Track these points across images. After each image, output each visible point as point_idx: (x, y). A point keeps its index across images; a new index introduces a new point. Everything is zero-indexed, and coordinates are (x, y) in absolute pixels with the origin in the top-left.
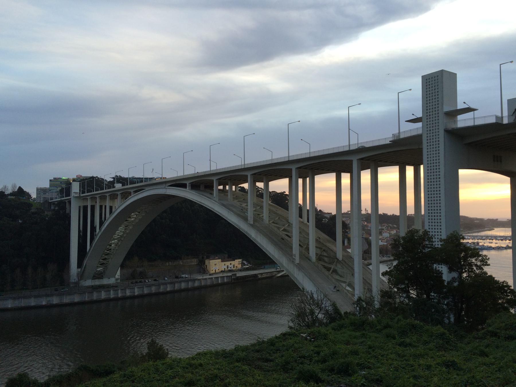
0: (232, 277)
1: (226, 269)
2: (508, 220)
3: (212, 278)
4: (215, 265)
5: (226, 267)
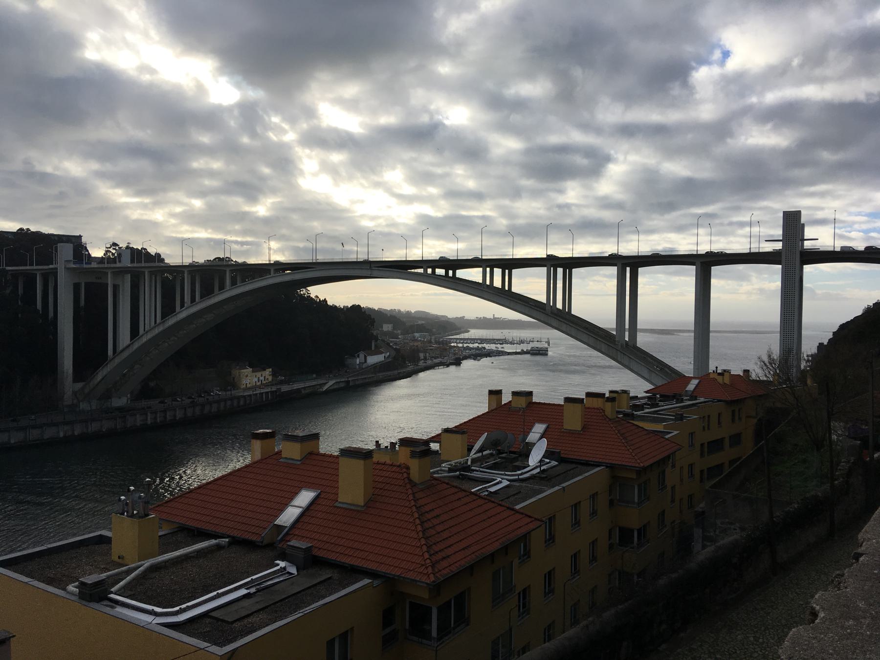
0: (276, 393)
1: (257, 382)
3: (257, 394)
4: (247, 376)
5: (256, 380)
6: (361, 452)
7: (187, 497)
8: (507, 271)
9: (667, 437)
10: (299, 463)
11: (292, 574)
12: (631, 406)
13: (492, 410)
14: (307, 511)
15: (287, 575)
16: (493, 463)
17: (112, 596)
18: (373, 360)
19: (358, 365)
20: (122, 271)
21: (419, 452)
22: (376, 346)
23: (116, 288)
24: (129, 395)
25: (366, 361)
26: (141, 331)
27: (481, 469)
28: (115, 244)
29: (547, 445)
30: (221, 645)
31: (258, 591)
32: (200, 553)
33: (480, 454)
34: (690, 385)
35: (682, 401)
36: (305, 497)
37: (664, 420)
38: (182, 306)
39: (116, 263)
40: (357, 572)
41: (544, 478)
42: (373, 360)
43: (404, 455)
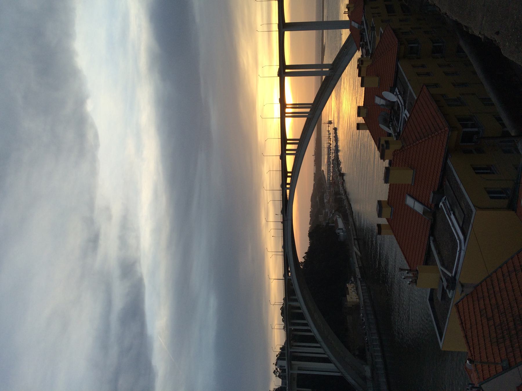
2: (315, 166)
6: (386, 171)
7: (411, 264)
8: (288, 142)
9: (382, 32)
10: (393, 208)
11: (445, 198)
12: (367, 57)
13: (368, 127)
14: (416, 199)
15: (446, 201)
16: (396, 121)
17: (453, 275)
18: (341, 224)
19: (344, 233)
20: (290, 366)
21: (386, 144)
22: (333, 223)
23: (299, 369)
24: (364, 366)
25: (342, 229)
26: (325, 356)
27: (399, 126)
28: (274, 372)
29: (385, 91)
30: (472, 211)
31: (452, 210)
32: (437, 248)
33: (391, 128)
34: (355, 26)
35: (364, 29)
36: (410, 201)
37: (374, 37)
38: (310, 331)
39: (285, 370)
40: (445, 169)
41: (404, 93)
42: (341, 224)
43: (389, 153)
